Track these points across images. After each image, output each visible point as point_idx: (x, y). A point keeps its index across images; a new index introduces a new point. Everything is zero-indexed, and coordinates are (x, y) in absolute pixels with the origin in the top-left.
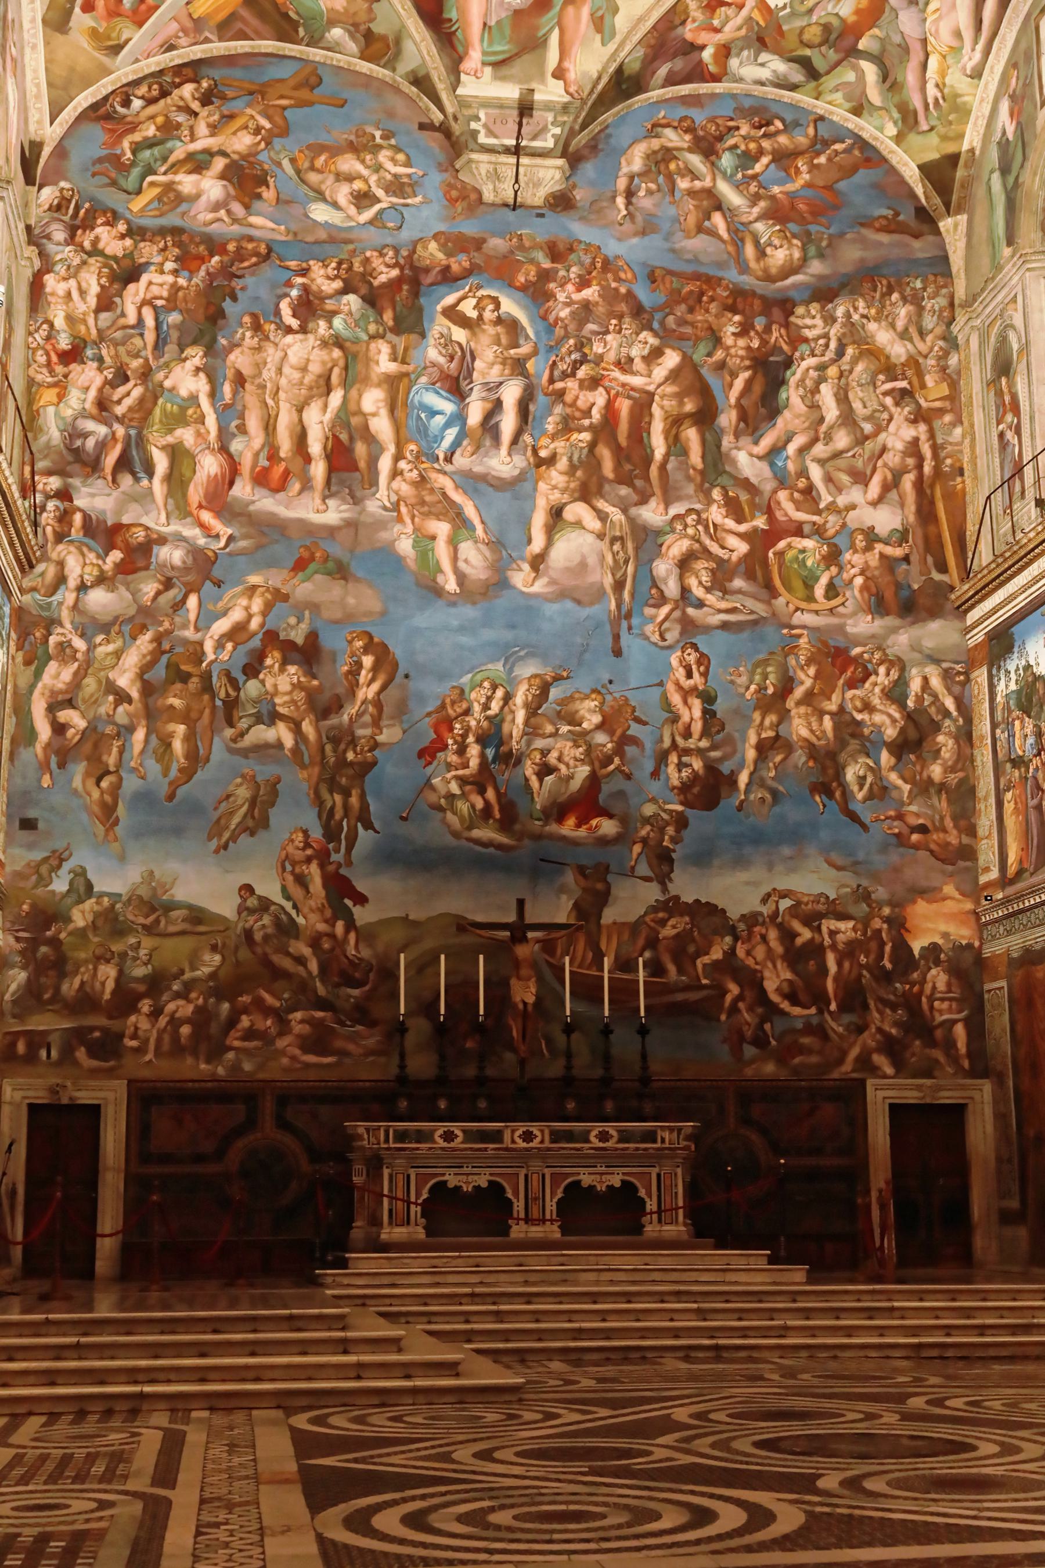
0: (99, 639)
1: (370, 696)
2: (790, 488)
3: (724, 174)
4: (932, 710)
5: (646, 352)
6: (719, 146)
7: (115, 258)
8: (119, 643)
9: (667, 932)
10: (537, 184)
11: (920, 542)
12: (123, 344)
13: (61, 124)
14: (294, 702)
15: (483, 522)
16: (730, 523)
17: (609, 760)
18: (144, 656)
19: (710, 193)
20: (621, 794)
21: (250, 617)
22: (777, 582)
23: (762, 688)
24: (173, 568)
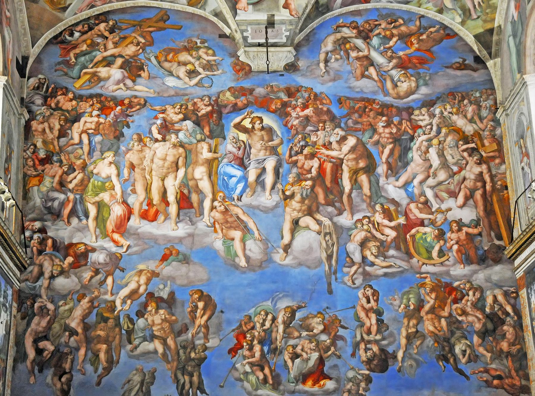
0: (61, 303)
1: (202, 323)
2: (416, 202)
3: (374, 48)
5: (338, 139)
6: (371, 34)
7: (67, 111)
8: (71, 304)
12: (72, 153)
13: (38, 47)
14: (163, 329)
15: (258, 230)
16: (386, 222)
17: (328, 349)
18: (84, 310)
19: (367, 57)
21: (139, 286)
22: (412, 250)
24: (99, 264)
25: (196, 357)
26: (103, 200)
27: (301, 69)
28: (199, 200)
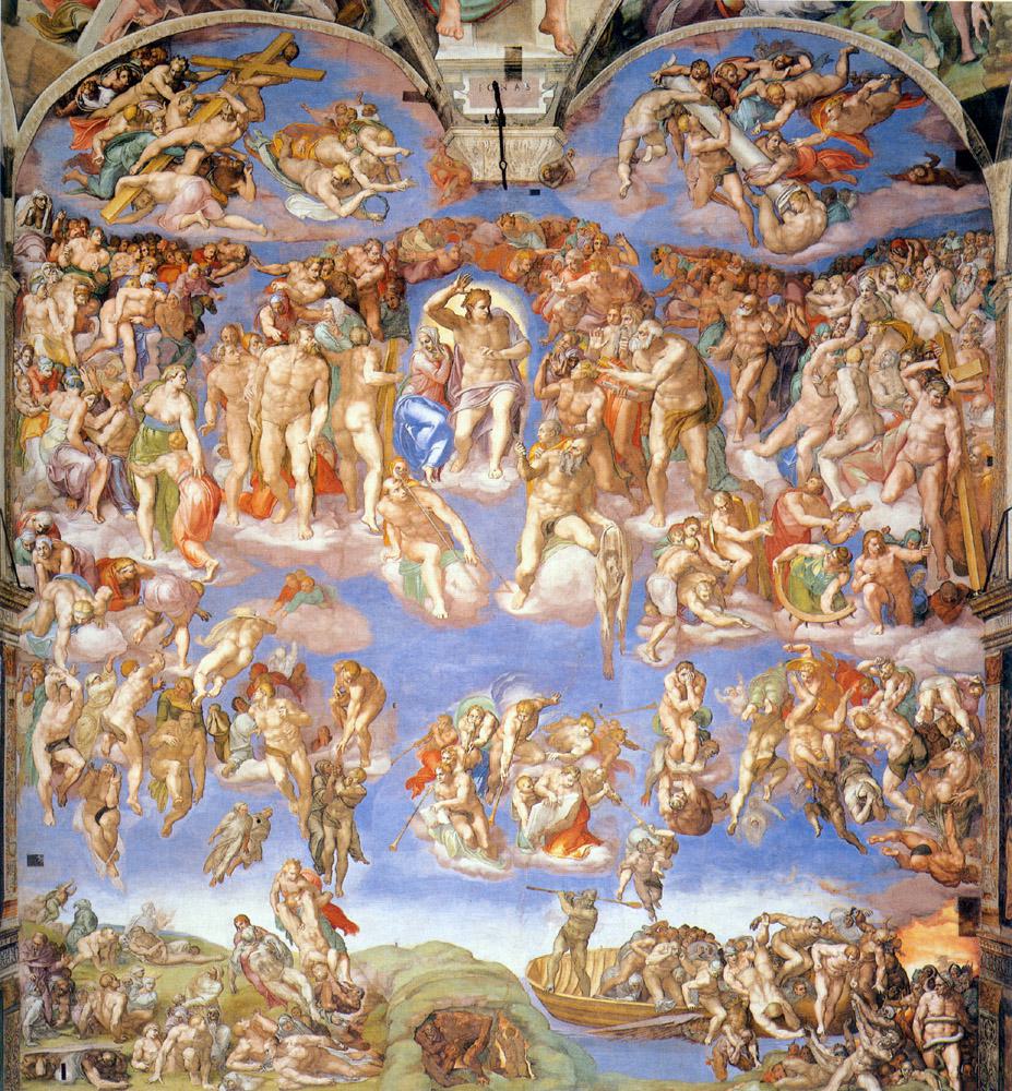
0: (91, 678)
3: (740, 127)
4: (942, 726)
5: (647, 344)
7: (91, 274)
9: (654, 957)
10: (531, 155)
11: (939, 543)
12: (103, 367)
14: (283, 735)
16: (733, 532)
17: (599, 786)
18: (137, 693)
19: (723, 151)
20: (610, 819)
21: (238, 650)
23: (760, 709)
24: (160, 602)
25: (345, 792)
26: (164, 471)
27: (577, 178)
28: (355, 475)
